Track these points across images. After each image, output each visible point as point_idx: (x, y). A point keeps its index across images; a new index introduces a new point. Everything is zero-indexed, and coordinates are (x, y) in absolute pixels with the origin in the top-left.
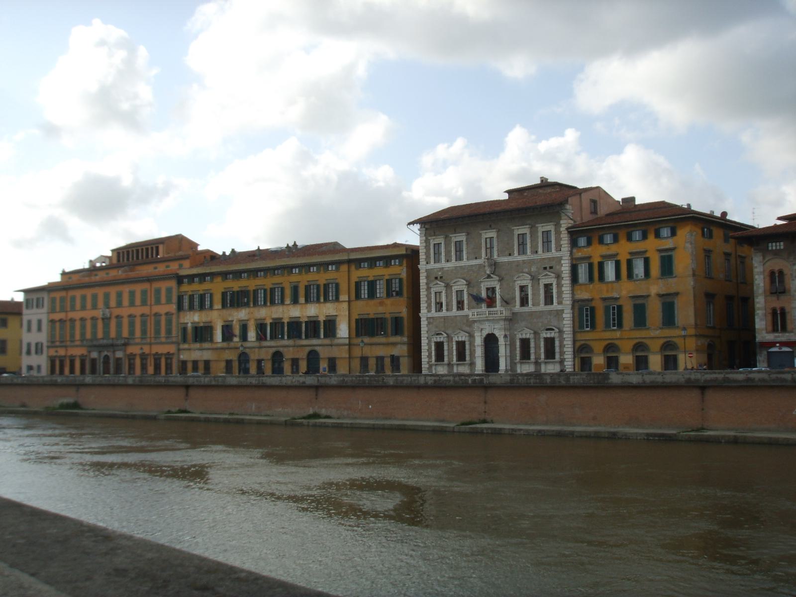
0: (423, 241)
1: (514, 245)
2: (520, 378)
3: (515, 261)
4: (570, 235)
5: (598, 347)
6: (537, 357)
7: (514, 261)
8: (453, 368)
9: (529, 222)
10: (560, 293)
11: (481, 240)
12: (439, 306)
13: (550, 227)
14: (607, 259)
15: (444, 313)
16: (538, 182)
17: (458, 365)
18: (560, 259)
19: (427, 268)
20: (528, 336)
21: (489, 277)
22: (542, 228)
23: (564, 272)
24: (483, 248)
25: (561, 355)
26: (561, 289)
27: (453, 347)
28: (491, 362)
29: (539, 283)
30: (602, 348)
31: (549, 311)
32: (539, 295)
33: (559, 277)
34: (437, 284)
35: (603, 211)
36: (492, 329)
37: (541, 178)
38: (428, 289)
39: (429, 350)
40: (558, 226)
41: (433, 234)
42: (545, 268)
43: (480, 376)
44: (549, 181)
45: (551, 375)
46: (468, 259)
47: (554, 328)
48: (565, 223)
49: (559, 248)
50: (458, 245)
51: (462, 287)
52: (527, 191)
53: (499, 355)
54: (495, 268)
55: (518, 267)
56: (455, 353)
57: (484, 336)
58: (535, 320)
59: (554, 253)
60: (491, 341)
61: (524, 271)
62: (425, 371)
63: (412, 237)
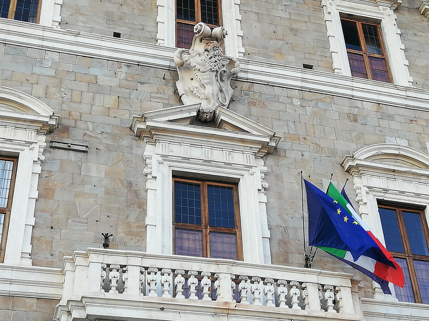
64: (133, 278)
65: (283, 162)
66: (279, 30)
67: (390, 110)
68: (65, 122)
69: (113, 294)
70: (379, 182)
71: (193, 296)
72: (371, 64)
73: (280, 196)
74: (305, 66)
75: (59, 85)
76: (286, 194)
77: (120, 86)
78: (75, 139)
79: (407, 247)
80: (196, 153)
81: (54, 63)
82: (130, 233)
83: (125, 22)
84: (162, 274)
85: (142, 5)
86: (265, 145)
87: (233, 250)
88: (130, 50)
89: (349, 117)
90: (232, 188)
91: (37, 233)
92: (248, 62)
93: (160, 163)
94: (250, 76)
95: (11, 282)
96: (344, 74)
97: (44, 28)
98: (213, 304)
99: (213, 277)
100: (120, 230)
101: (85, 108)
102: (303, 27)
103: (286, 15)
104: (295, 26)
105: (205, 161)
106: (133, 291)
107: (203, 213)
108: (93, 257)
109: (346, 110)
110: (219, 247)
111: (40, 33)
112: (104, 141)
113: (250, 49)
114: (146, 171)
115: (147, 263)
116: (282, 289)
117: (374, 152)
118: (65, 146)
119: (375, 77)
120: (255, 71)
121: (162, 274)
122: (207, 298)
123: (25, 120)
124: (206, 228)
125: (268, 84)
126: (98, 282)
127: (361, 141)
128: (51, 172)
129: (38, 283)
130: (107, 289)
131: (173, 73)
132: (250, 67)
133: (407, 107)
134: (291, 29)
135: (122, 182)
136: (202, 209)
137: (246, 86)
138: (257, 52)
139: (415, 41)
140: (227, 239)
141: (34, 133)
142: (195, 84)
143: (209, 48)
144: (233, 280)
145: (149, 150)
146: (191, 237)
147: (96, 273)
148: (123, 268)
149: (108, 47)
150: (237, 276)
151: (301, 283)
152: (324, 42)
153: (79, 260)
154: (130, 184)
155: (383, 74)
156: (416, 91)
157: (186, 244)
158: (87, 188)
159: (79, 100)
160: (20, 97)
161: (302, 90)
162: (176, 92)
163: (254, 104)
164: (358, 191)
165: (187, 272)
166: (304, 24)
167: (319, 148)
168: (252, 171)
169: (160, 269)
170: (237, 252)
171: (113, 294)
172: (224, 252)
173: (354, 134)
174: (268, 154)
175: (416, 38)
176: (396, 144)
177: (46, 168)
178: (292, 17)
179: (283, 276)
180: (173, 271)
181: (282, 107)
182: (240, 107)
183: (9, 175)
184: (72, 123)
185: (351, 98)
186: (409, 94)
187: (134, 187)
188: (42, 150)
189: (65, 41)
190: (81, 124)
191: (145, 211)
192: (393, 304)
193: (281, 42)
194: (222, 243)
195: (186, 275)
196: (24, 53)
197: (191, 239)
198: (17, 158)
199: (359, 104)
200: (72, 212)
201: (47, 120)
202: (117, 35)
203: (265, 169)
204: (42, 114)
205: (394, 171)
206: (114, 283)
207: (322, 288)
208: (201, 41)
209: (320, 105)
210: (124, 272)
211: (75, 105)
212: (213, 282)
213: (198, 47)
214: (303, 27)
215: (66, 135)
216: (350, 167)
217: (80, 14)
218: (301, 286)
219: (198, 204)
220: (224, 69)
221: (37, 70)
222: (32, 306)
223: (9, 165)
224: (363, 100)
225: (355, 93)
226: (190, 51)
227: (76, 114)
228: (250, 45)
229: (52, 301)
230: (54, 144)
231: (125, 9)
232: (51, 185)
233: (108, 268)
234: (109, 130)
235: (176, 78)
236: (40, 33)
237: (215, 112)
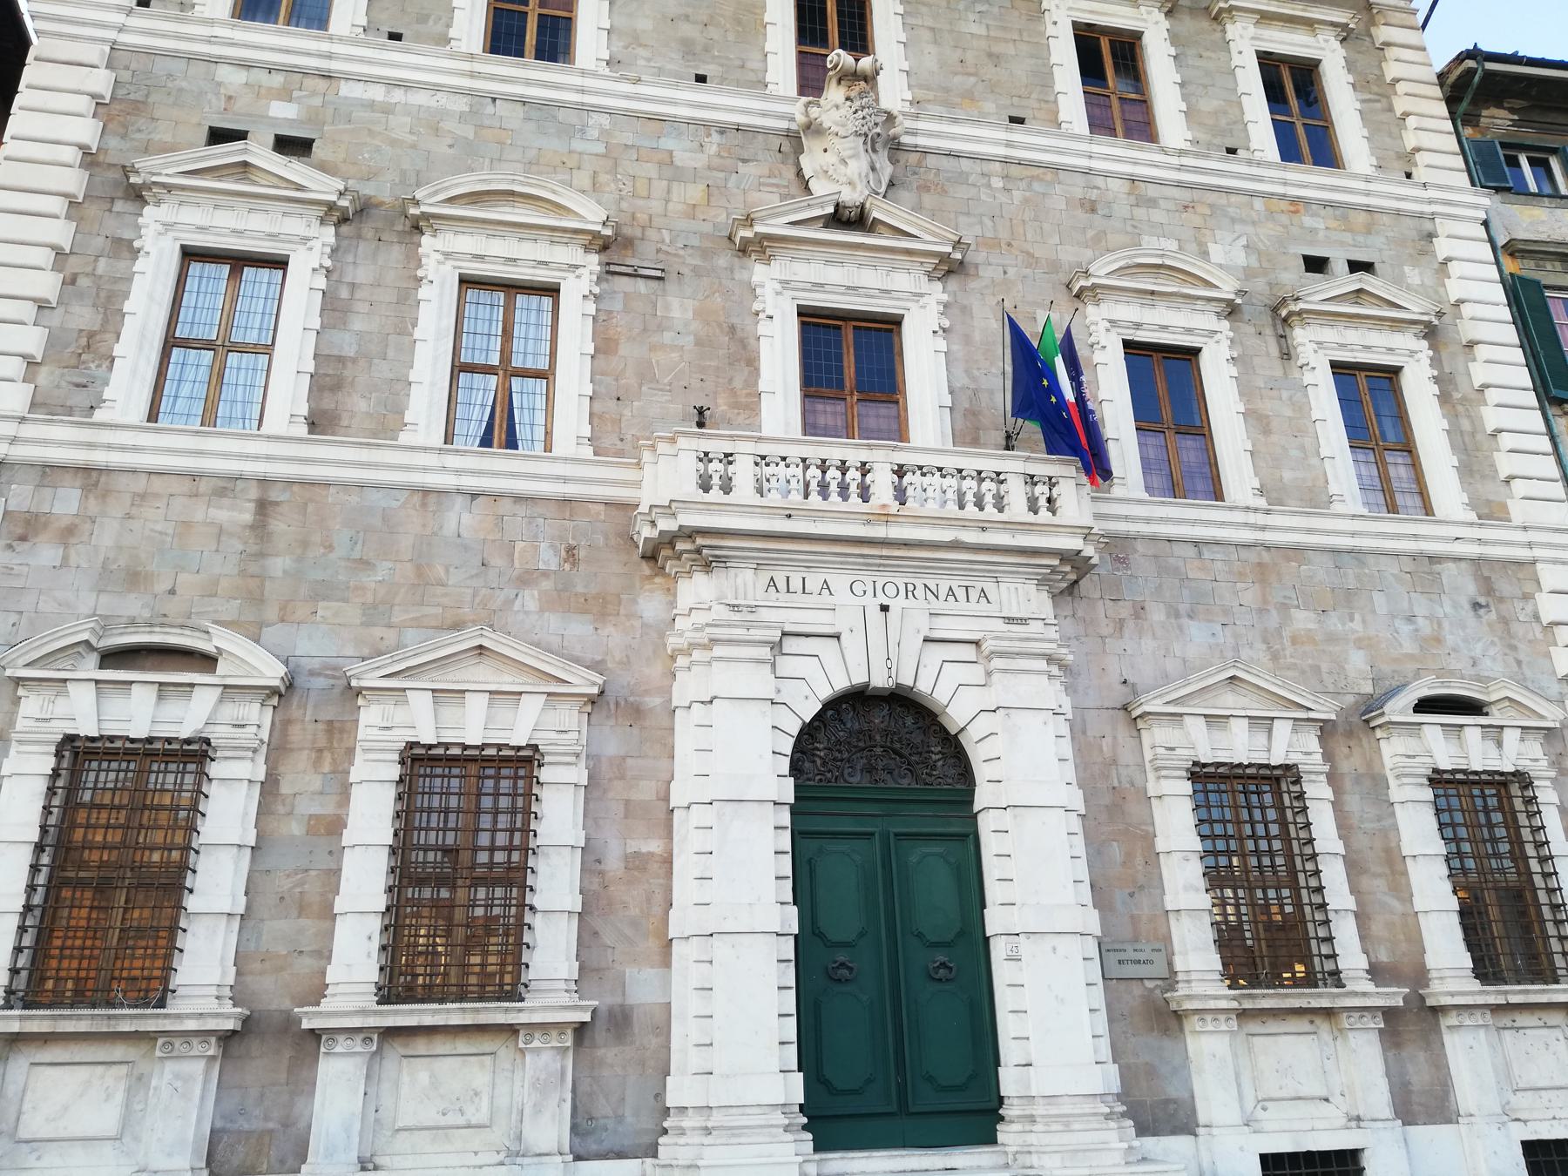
6: (1383, 956)
15: (272, 427)
19: (125, 38)
26: (1477, 422)
27: (335, 826)
31: (1414, 557)
53: (994, 920)
58: (1303, 620)
64: (743, 472)
65: (973, 284)
66: (970, 57)
67: (1152, 191)
68: (627, 231)
69: (715, 495)
70: (1129, 312)
71: (834, 497)
72: (1123, 112)
73: (967, 340)
74: (1013, 120)
75: (614, 170)
76: (977, 337)
77: (709, 168)
78: (644, 257)
79: (1167, 413)
80: (834, 275)
81: (603, 132)
82: (736, 405)
83: (714, 57)
84: (787, 466)
85: (739, 22)
86: (944, 258)
87: (895, 427)
88: (726, 104)
89: (1082, 205)
90: (891, 331)
91: (597, 406)
92: (917, 117)
93: (778, 293)
94: (921, 141)
95: (565, 480)
96: (1077, 131)
97: (583, 73)
98: (865, 508)
99: (864, 469)
100: (720, 401)
101: (656, 206)
102: (1009, 49)
103: (980, 30)
104: (996, 49)
105: (849, 288)
106: (744, 490)
107: (846, 371)
108: (682, 442)
109: (1078, 193)
110: (872, 423)
111: (577, 81)
112: (690, 261)
113: (921, 94)
114: (756, 306)
115: (763, 449)
116: (970, 485)
117: (1122, 263)
118: (629, 270)
119: (1128, 134)
120: (930, 132)
121: (787, 466)
122: (854, 499)
123: (565, 230)
124: (852, 394)
125: (950, 154)
126: (694, 479)
127: (1100, 244)
128: (611, 312)
129: (602, 481)
130: (706, 488)
131: (794, 141)
132: (921, 125)
133: (1179, 185)
134: (990, 55)
135: (720, 325)
136: (845, 364)
137: (913, 158)
138: (931, 97)
139: (1198, 67)
140: (884, 410)
141: (581, 251)
142: (831, 158)
143: (853, 94)
144: (894, 472)
145: (761, 273)
146: (829, 408)
147: (689, 467)
148: (728, 458)
149: (686, 101)
150: (901, 466)
151: (998, 474)
152: (1044, 78)
153: (662, 447)
154: (733, 329)
155: (1142, 128)
156: (1197, 155)
157: (821, 420)
158: (668, 337)
159: (645, 194)
160: (554, 192)
161: (1006, 161)
162: (799, 172)
163: (928, 189)
164: (1092, 328)
165: (824, 461)
166: (1011, 45)
167: (1031, 260)
168: (923, 301)
169: (784, 459)
170: (900, 430)
171: (715, 495)
172: (880, 431)
173: (1090, 233)
174: (949, 272)
175: (1199, 63)
176: (1155, 247)
177: (602, 306)
178: (992, 34)
179: (970, 464)
180: (804, 460)
181: (973, 192)
182: (905, 195)
183: (547, 318)
184: (638, 232)
185: (1088, 172)
186: (1186, 161)
187: (739, 334)
188: (595, 278)
189: (616, 93)
190: (651, 233)
191: (757, 370)
192: (1140, 502)
193: (972, 79)
194: (878, 416)
195: (823, 466)
196: (554, 117)
197: (828, 412)
198: (558, 291)
199: (1100, 181)
200: (646, 374)
201: (598, 228)
202: (701, 79)
203: (945, 297)
204: (590, 217)
205: (1153, 293)
206: (716, 480)
207: (1031, 480)
208: (839, 82)
209: (1036, 186)
210: (730, 463)
211: (641, 202)
212: (864, 475)
213: (835, 93)
214: (1009, 49)
215: (630, 253)
216: (1082, 289)
217: (640, 45)
218: (999, 478)
219: (839, 358)
220: (878, 130)
221: (578, 145)
222: (598, 514)
223: (547, 302)
224: (1107, 175)
225: (1095, 164)
226: (822, 101)
227: (642, 217)
228: (921, 87)
229: (628, 507)
230: (612, 268)
231: (713, 33)
232: (612, 332)
233: (706, 457)
234: (695, 242)
235: (799, 149)
236: (577, 81)
237: (863, 206)
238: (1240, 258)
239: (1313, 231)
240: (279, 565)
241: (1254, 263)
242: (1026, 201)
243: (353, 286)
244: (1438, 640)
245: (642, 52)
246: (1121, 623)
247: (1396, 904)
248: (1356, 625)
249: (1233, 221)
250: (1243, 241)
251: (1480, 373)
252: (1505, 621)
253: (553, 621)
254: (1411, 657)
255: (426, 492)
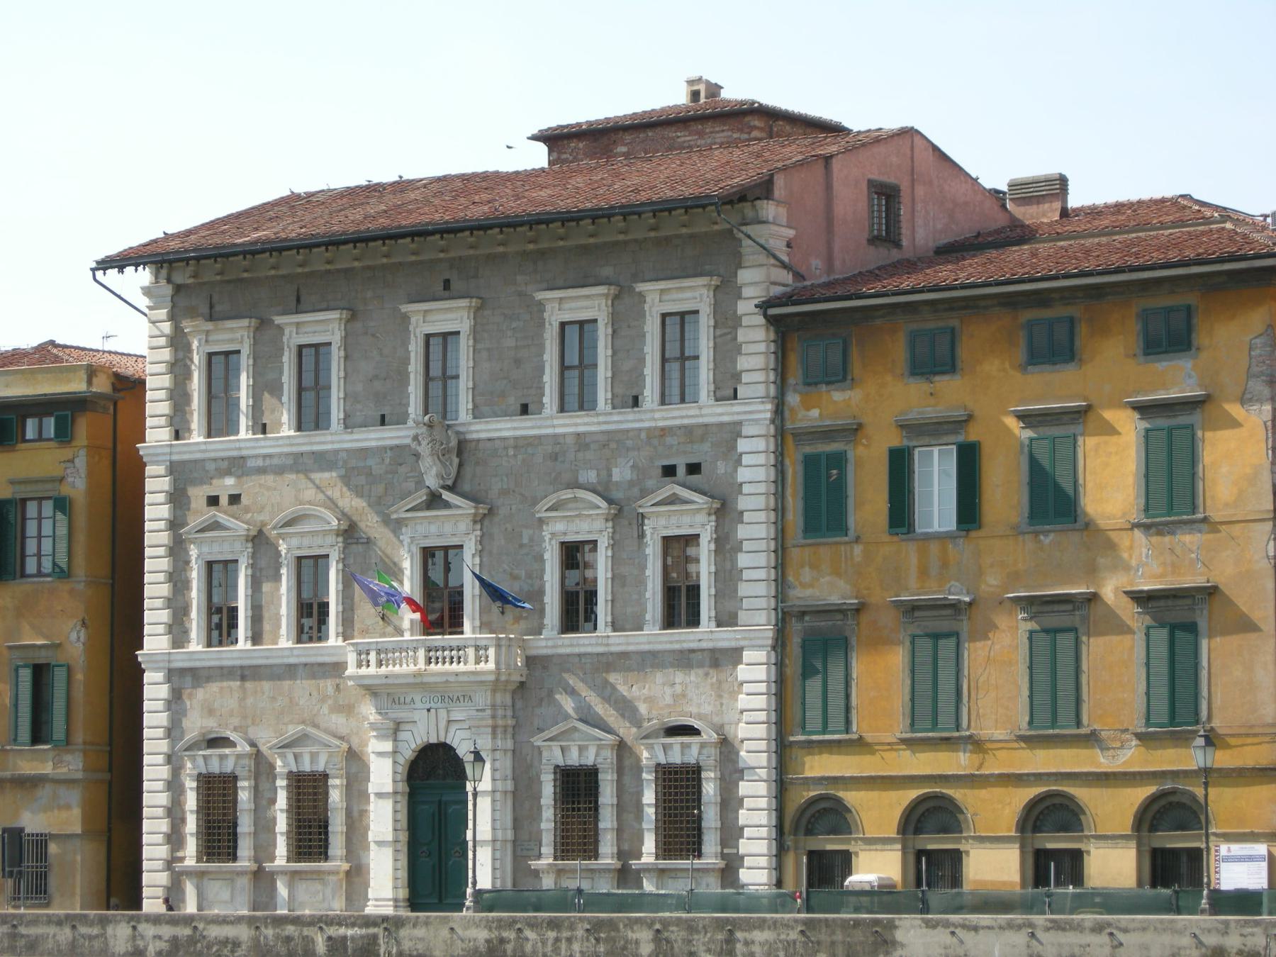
0: (162, 341)
1: (540, 370)
2: (529, 934)
3: (547, 436)
4: (776, 333)
5: (878, 812)
6: (626, 847)
7: (539, 437)
8: (274, 888)
9: (607, 271)
10: (727, 578)
11: (405, 343)
12: (222, 624)
13: (694, 294)
14: (926, 440)
16: (675, 96)
17: (294, 876)
18: (733, 431)
19: (175, 458)
20: (590, 759)
21: (434, 501)
22: (661, 298)
23: (746, 489)
24: (412, 376)
25: (724, 843)
26: (734, 561)
28: (434, 869)
29: (642, 535)
30: (897, 814)
31: (681, 651)
32: (641, 582)
33: (725, 510)
34: (216, 526)
35: (923, 227)
36: (442, 724)
37: (691, 82)
38: (177, 550)
39: (174, 813)
40: (727, 291)
41: (205, 309)
42: (669, 471)
43: (360, 927)
44: (725, 94)
45: (658, 926)
46: (348, 424)
47: (696, 724)
48: (756, 281)
49: (727, 390)
50: (312, 358)
51: (319, 541)
52: (628, 137)
54: (460, 465)
55: (559, 465)
56: (282, 824)
57: (408, 753)
59: (706, 410)
60: (434, 780)
61: (582, 480)
62: (152, 904)
63: (123, 325)
77: (387, 472)
81: (345, 462)
109: (549, 449)
209: (530, 450)
236: (329, 438)
238: (628, 474)
239: (671, 446)
240: (250, 701)
241: (635, 477)
242: (524, 460)
243: (261, 570)
244: (684, 696)
245: (359, 406)
246: (542, 700)
247: (635, 824)
248: (645, 691)
249: (628, 450)
250: (631, 463)
251: (742, 532)
252: (720, 682)
253: (334, 717)
254: (669, 706)
255: (290, 665)
